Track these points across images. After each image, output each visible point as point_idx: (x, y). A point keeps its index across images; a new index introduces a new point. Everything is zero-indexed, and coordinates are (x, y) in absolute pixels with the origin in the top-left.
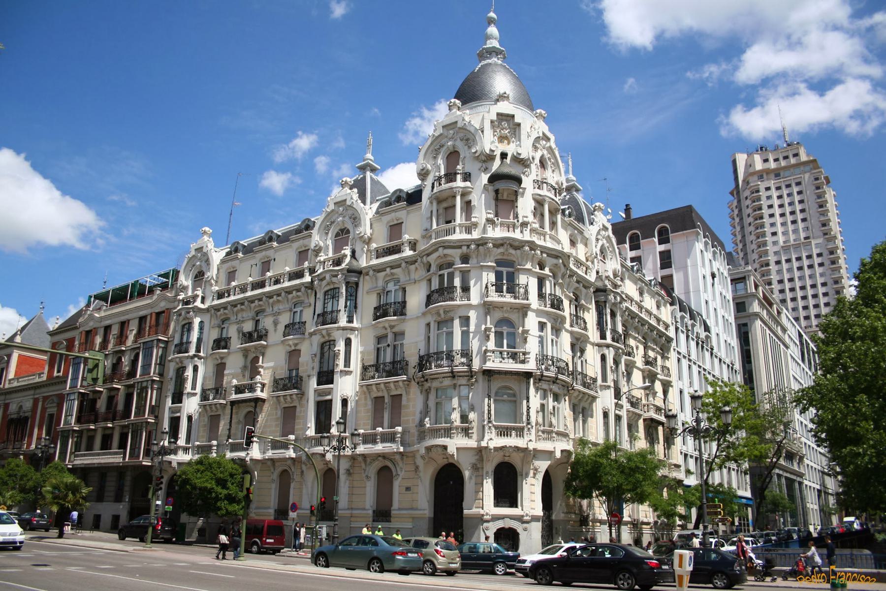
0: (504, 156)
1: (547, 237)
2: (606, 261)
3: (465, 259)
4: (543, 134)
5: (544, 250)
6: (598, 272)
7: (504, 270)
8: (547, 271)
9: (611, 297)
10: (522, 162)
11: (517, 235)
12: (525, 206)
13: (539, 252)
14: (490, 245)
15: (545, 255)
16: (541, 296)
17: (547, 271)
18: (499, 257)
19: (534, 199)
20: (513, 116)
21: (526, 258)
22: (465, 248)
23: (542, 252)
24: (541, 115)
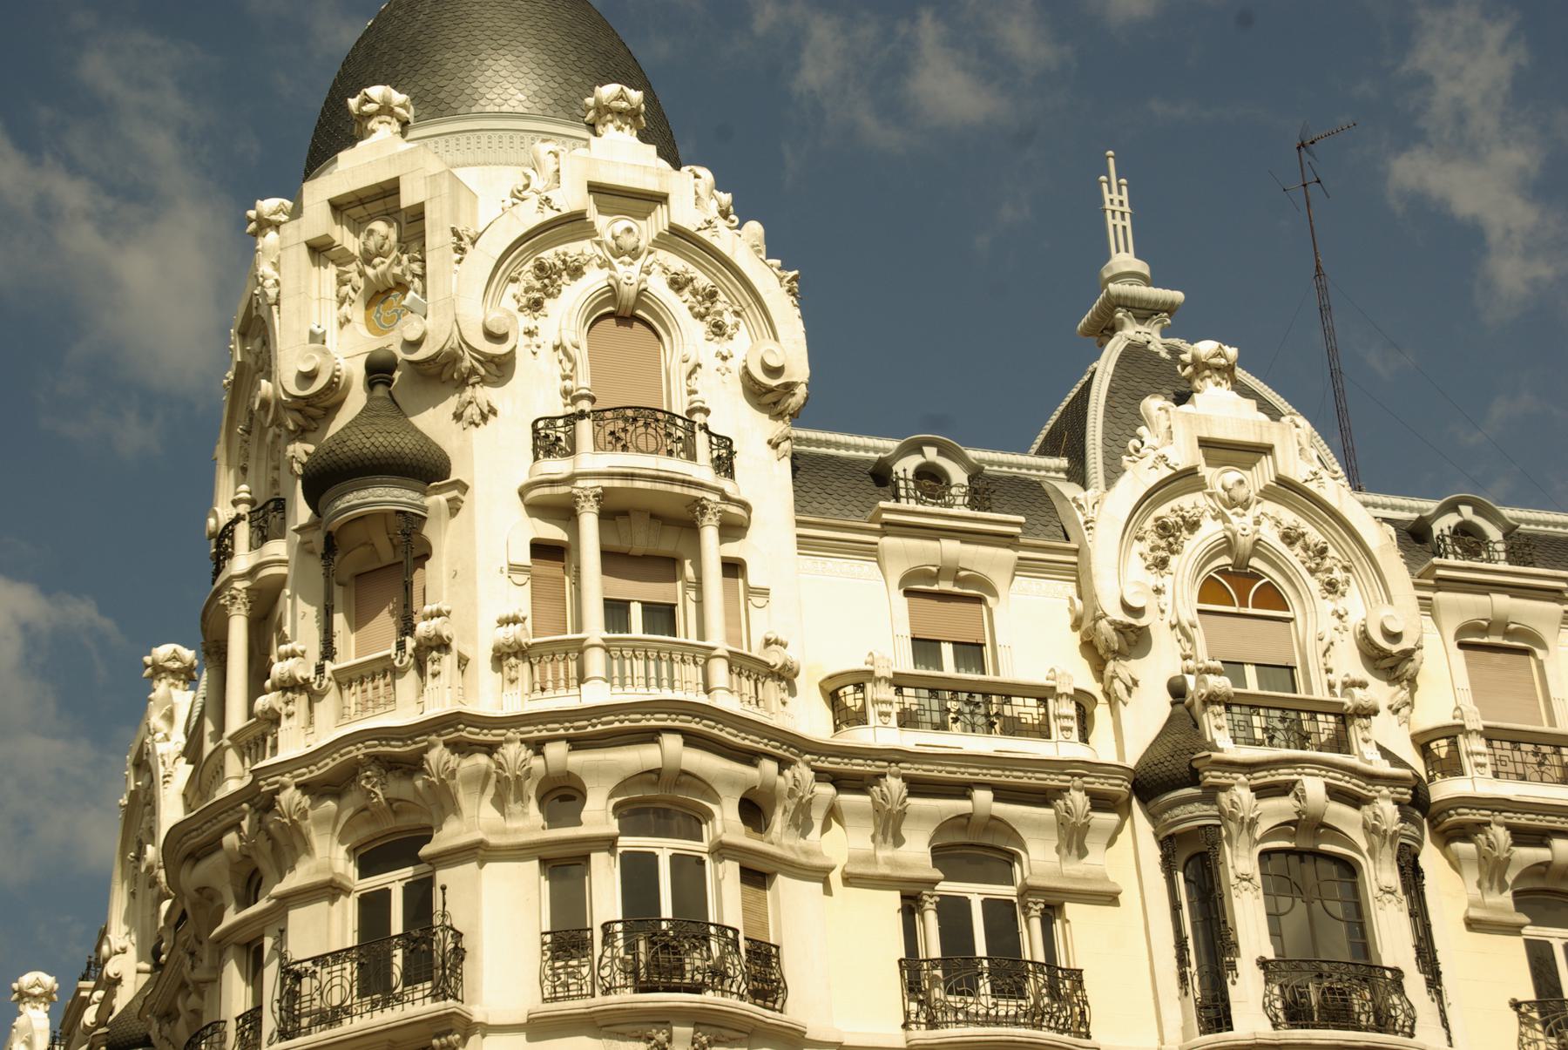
0: (379, 370)
1: (596, 662)
2: (1295, 611)
3: (250, 889)
4: (595, 189)
5: (536, 729)
6: (1177, 691)
7: (395, 881)
8: (598, 815)
9: (1241, 795)
10: (442, 374)
11: (407, 706)
12: (479, 564)
13: (514, 753)
14: (291, 798)
15: (557, 752)
16: (567, 941)
17: (598, 815)
18: (364, 832)
19: (538, 509)
20: (390, 190)
21: (443, 801)
22: (231, 839)
23: (537, 746)
24: (603, 110)
